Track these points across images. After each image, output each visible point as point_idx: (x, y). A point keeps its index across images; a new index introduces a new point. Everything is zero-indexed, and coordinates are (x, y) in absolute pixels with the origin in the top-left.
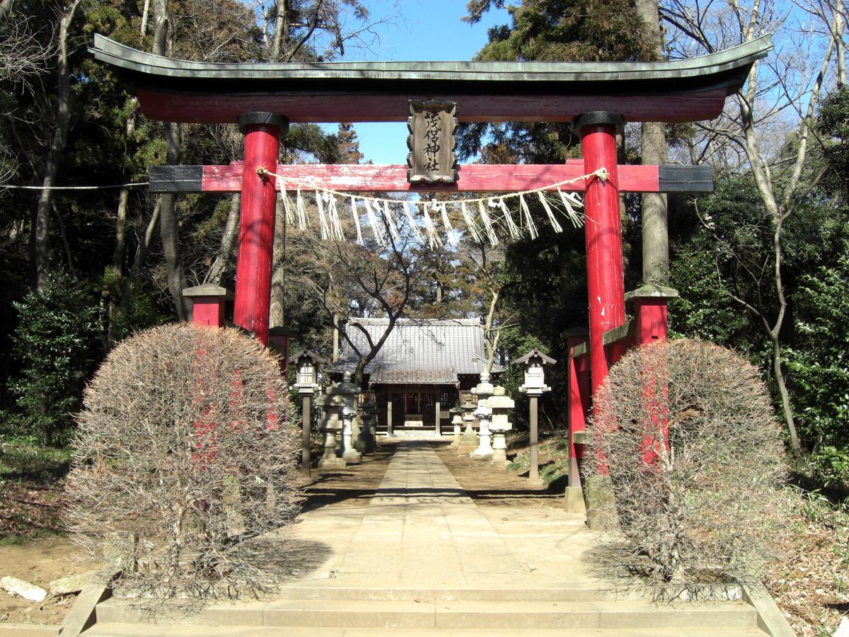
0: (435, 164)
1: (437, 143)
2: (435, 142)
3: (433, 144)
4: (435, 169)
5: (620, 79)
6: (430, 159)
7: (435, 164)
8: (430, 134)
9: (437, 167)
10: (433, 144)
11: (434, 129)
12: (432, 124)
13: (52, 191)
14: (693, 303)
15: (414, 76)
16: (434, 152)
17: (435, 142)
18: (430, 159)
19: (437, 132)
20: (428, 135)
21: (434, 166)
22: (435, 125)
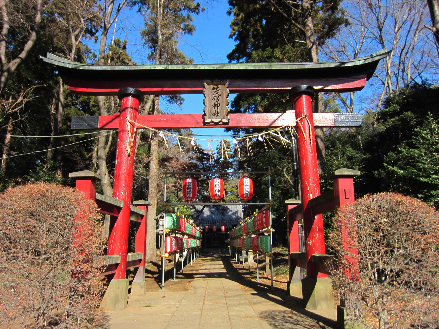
0: (218, 113)
1: (219, 102)
2: (218, 102)
3: (216, 103)
4: (218, 116)
5: (313, 67)
6: (215, 111)
7: (218, 113)
8: (215, 98)
9: (219, 114)
10: (216, 103)
11: (217, 95)
12: (216, 92)
13: (50, 135)
14: (434, 183)
15: (206, 67)
16: (218, 107)
17: (218, 102)
18: (215, 111)
19: (218, 96)
20: (214, 98)
21: (218, 114)
22: (217, 93)
